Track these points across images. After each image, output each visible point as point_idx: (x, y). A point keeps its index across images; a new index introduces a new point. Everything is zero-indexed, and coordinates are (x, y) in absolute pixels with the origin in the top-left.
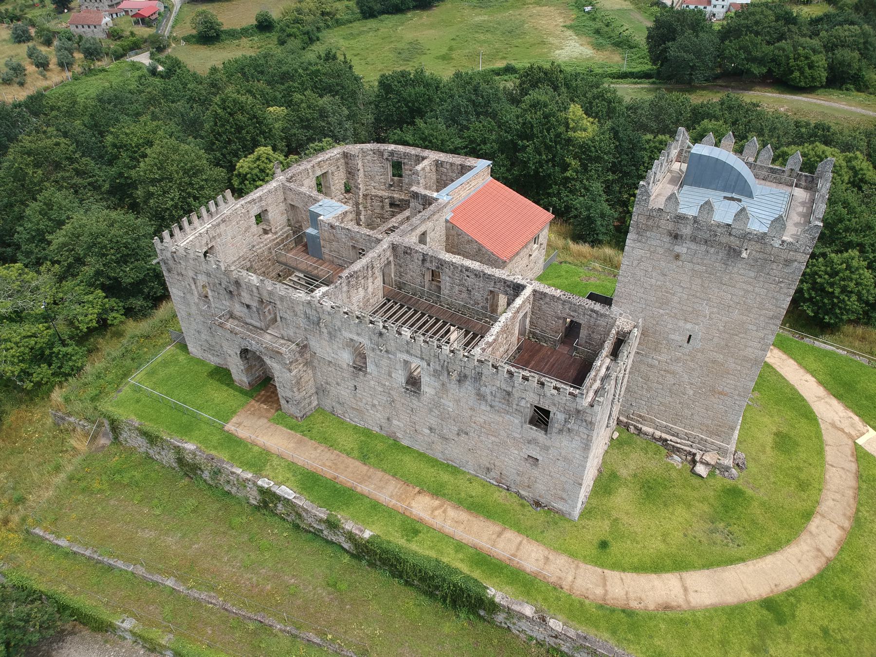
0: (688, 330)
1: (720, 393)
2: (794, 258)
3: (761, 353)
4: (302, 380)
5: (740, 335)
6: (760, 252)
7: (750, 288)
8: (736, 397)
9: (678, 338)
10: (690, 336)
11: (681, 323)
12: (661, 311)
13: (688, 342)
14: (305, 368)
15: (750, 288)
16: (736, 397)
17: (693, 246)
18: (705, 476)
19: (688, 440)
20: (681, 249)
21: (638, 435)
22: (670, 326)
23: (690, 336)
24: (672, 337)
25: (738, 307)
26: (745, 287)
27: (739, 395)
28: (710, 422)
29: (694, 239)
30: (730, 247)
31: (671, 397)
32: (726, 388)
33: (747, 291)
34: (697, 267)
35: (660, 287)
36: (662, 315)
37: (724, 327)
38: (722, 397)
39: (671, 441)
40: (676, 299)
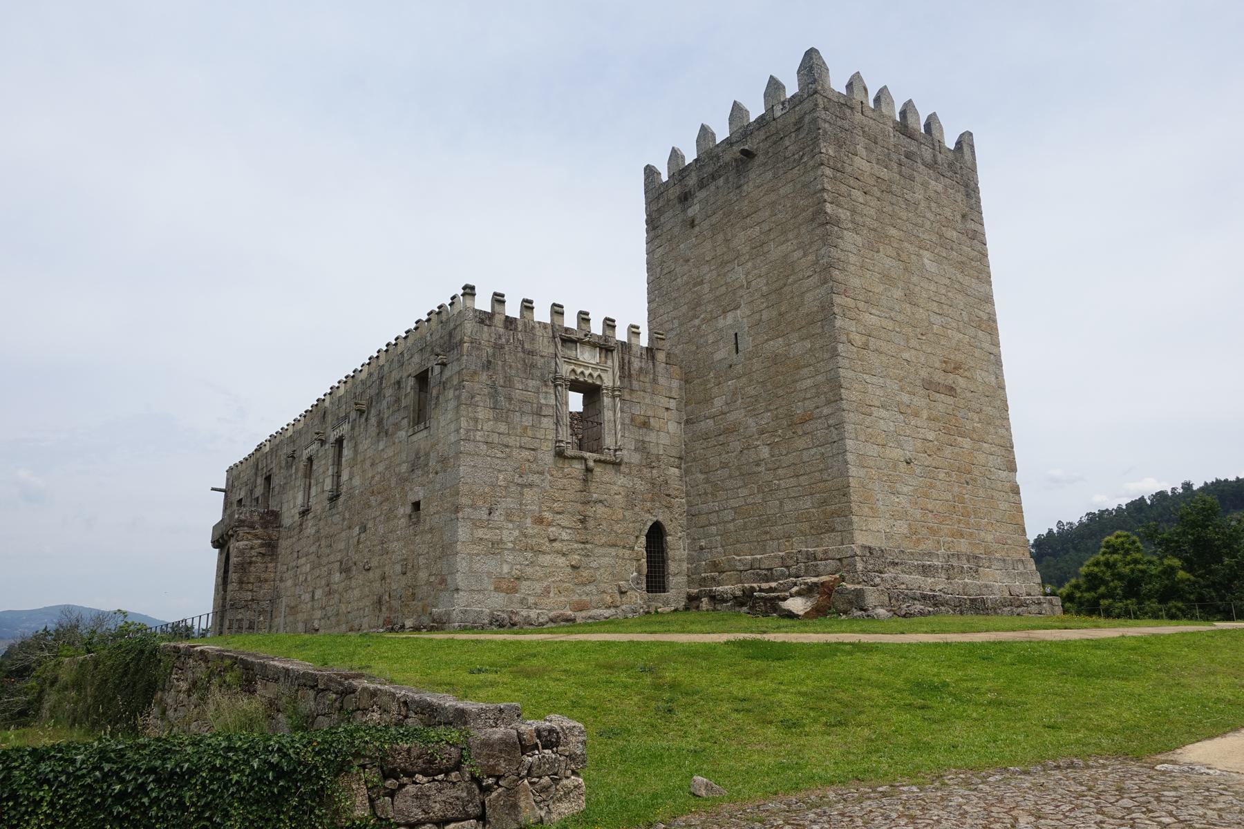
0: (731, 327)
1: (804, 422)
2: (803, 112)
3: (822, 291)
4: (252, 569)
5: (790, 281)
6: (766, 139)
7: (773, 197)
8: (826, 411)
9: (723, 353)
10: (736, 334)
11: (721, 323)
12: (697, 322)
13: (737, 352)
14: (263, 550)
15: (773, 197)
16: (826, 411)
17: (701, 195)
18: (802, 613)
19: (789, 576)
20: (694, 210)
21: (715, 610)
22: (711, 339)
23: (736, 334)
24: (718, 356)
25: (772, 237)
26: (767, 199)
27: (828, 402)
28: (809, 504)
29: (702, 185)
30: (736, 160)
31: (745, 485)
32: (807, 402)
33: (774, 203)
34: (714, 219)
35: (687, 283)
36: (699, 327)
37: (767, 284)
38: (808, 427)
39: (761, 590)
40: (706, 287)
